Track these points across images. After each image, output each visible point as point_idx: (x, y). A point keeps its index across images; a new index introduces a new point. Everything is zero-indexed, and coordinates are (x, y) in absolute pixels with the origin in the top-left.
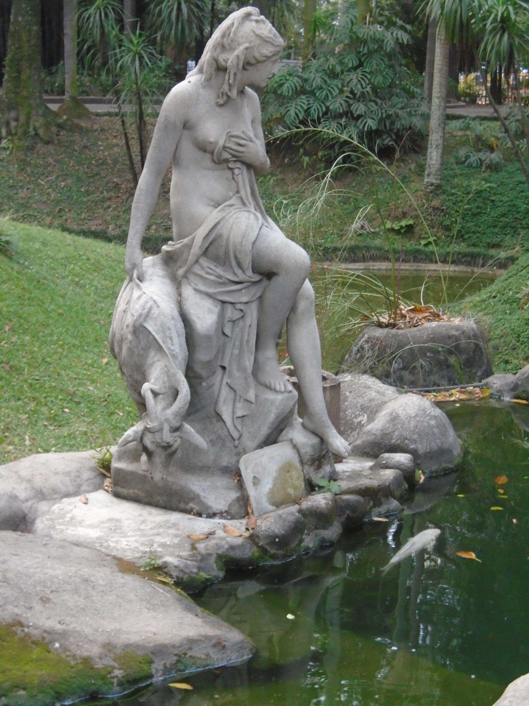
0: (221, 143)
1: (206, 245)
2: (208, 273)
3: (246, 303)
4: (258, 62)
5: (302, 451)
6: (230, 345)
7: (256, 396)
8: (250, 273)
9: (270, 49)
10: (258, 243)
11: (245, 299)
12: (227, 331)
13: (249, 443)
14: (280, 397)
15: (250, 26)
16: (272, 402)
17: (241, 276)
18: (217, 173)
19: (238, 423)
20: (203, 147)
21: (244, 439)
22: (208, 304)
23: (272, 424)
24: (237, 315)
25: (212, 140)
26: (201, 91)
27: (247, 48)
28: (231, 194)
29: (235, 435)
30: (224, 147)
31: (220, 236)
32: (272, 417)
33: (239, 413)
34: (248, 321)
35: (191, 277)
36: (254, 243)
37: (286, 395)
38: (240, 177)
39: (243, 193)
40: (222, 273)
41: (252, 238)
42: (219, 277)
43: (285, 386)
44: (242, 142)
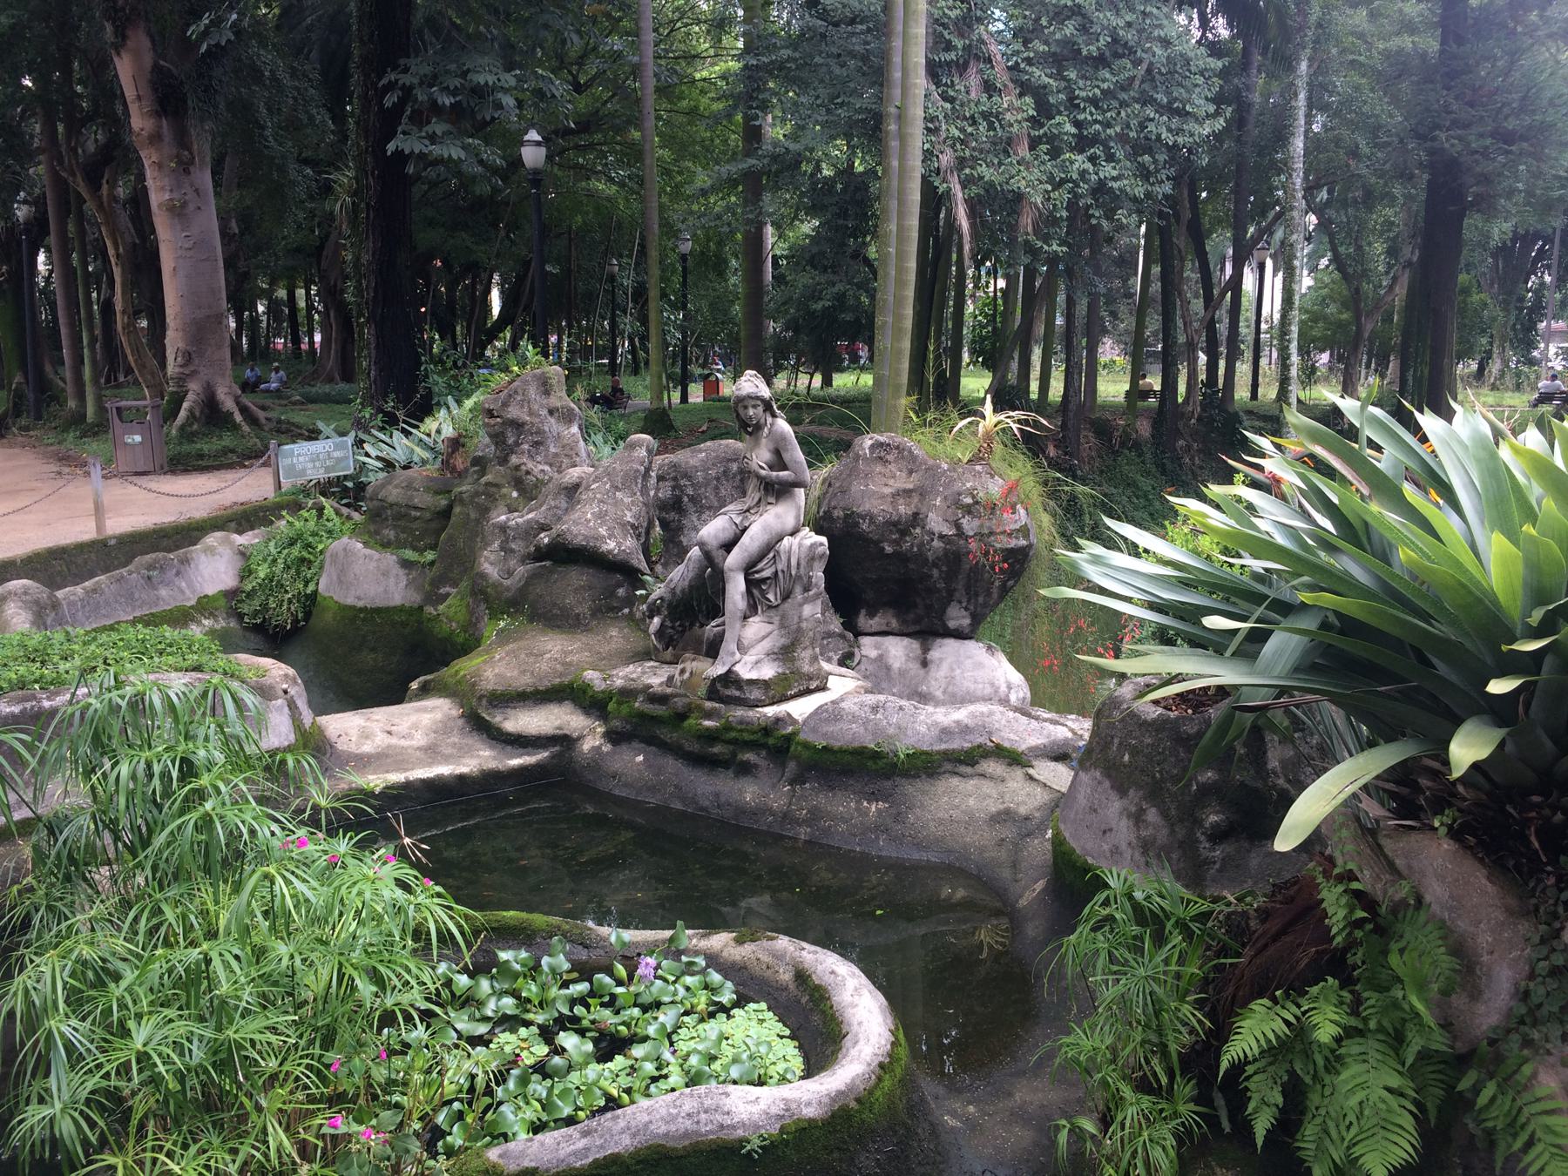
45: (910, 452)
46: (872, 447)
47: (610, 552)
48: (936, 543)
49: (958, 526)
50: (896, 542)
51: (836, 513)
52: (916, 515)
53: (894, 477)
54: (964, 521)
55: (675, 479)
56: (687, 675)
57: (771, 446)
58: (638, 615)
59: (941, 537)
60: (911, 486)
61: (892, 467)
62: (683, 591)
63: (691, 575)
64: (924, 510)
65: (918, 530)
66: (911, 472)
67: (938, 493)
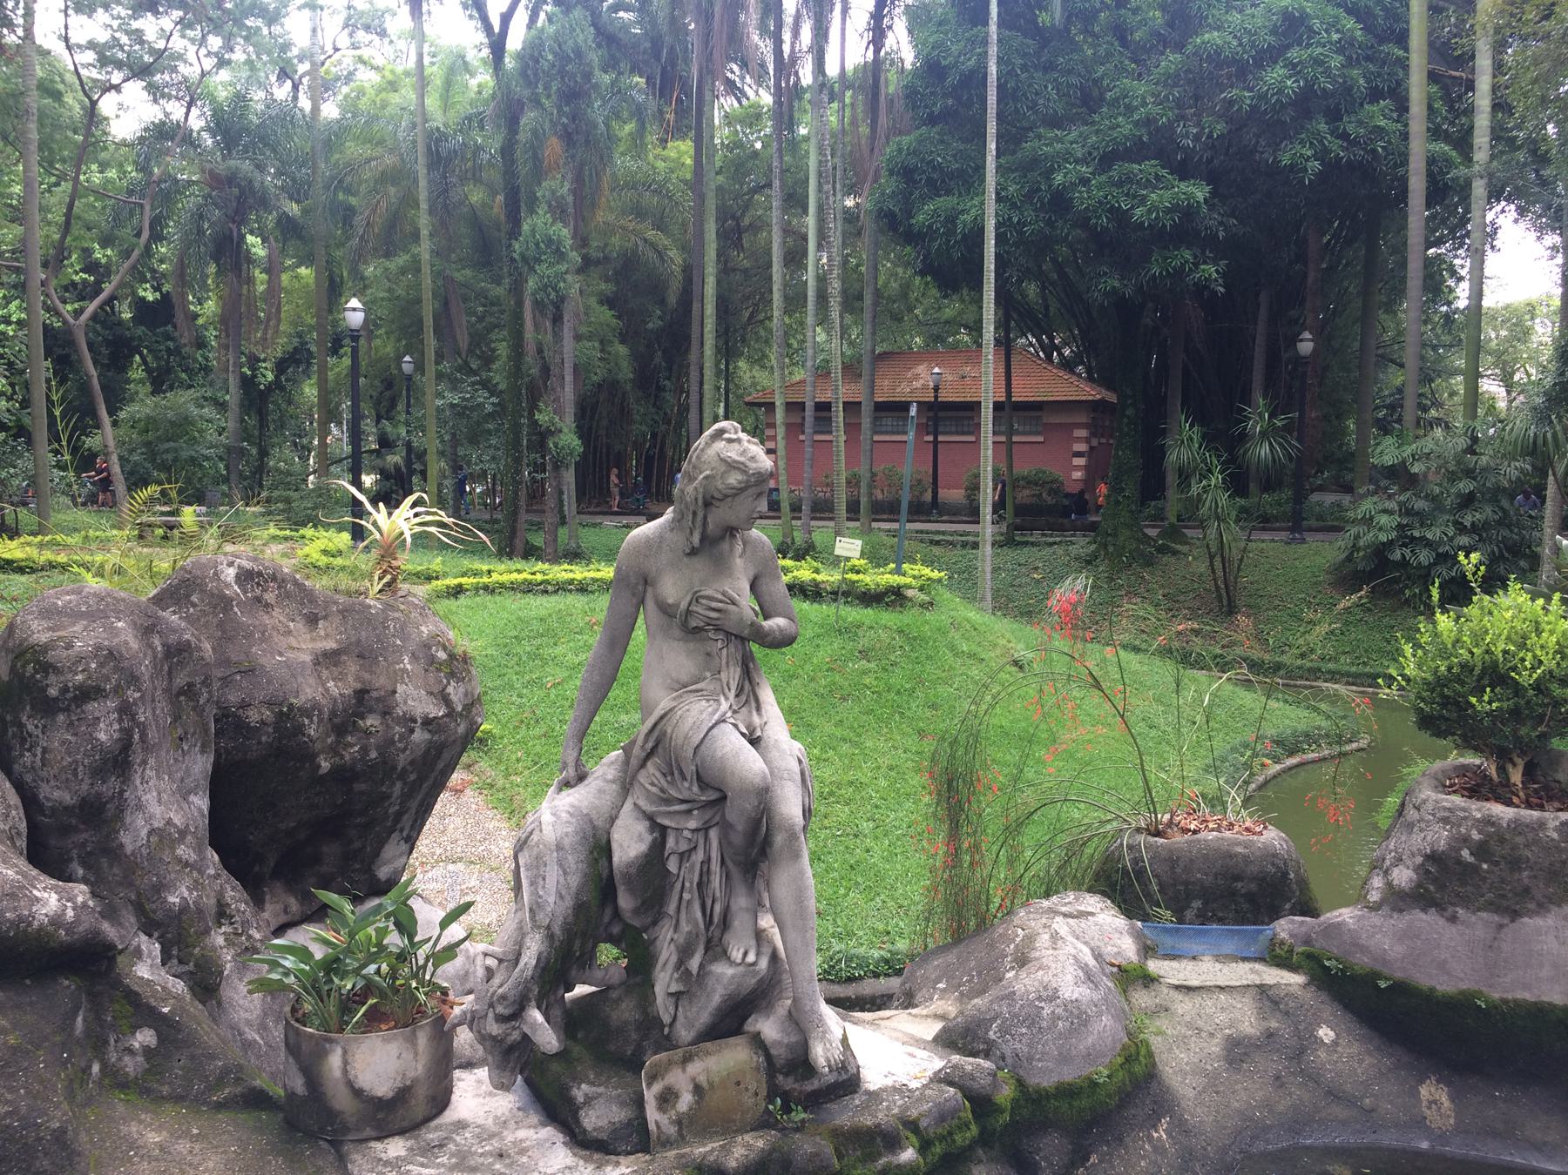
0: (684, 605)
1: (650, 745)
2: (652, 784)
3: (693, 831)
4: (727, 496)
5: (773, 1052)
6: (678, 886)
7: (701, 966)
8: (695, 789)
9: (740, 477)
10: (703, 748)
11: (693, 824)
12: (672, 866)
13: (684, 1034)
14: (730, 971)
15: (719, 445)
16: (719, 977)
17: (685, 795)
18: (691, 645)
19: (671, 1002)
20: (665, 610)
21: (678, 1025)
22: (641, 827)
23: (719, 1009)
24: (684, 847)
25: (670, 601)
26: (668, 535)
27: (706, 478)
28: (708, 674)
29: (666, 1019)
30: (688, 612)
31: (664, 733)
32: (716, 999)
33: (674, 988)
34: (699, 856)
35: (636, 786)
36: (698, 747)
37: (741, 968)
38: (725, 651)
39: (723, 675)
40: (665, 785)
41: (696, 740)
42: (662, 790)
43: (745, 954)
44: (714, 605)
45: (296, 582)
46: (238, 577)
47: (56, 920)
48: (419, 736)
49: (446, 700)
50: (334, 751)
51: (253, 716)
52: (361, 694)
53: (290, 632)
54: (450, 689)
55: (117, 690)
56: (685, 1101)
57: (751, 574)
58: (132, 1066)
59: (428, 722)
60: (331, 645)
61: (276, 612)
62: (568, 928)
63: (574, 881)
64: (381, 681)
65: (372, 721)
66: (312, 620)
67: (399, 651)
